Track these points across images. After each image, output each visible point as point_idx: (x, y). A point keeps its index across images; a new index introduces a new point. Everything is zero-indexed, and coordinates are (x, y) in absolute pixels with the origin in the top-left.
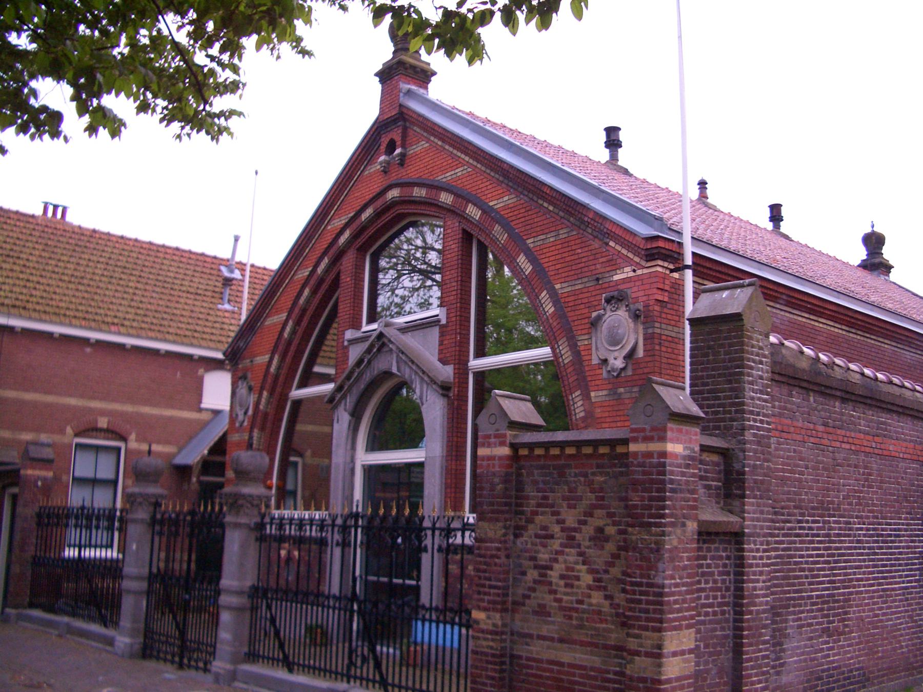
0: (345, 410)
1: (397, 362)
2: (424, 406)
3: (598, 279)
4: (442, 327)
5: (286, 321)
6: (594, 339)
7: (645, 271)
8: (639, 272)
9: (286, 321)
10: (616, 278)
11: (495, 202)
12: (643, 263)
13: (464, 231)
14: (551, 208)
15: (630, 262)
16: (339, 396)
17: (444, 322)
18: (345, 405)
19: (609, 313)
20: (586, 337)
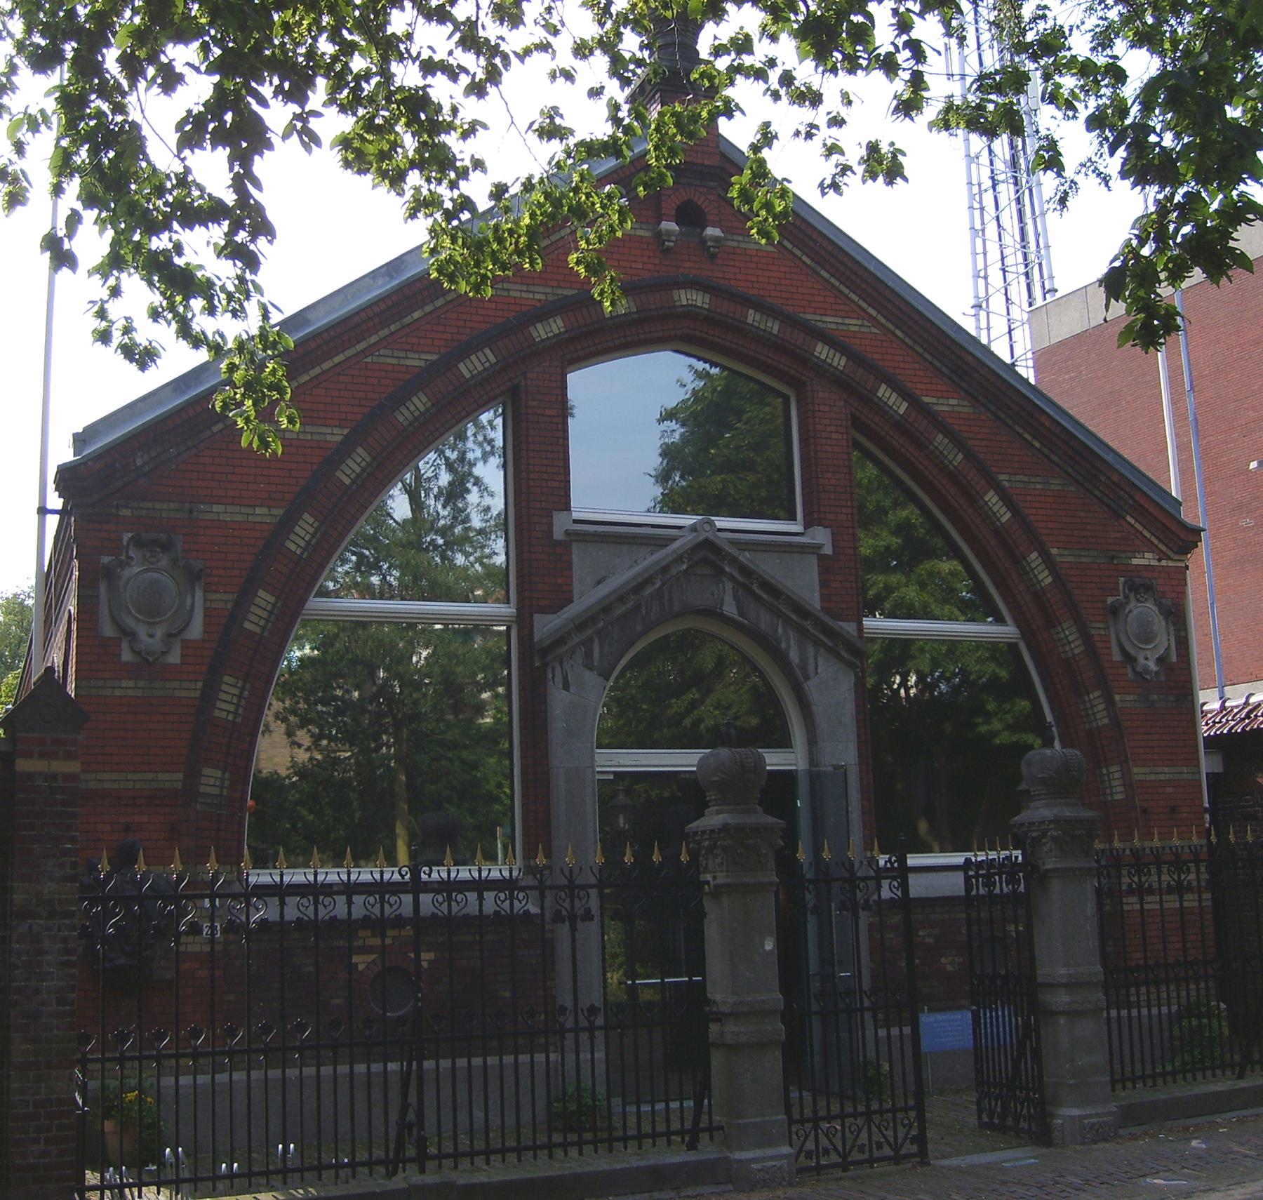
0: (589, 666)
1: (736, 598)
2: (810, 682)
3: (1113, 557)
4: (822, 558)
5: (345, 449)
6: (1112, 630)
7: (1171, 563)
8: (1164, 563)
9: (345, 449)
10: (1135, 562)
11: (934, 400)
12: (1170, 554)
13: (852, 415)
14: (1037, 445)
15: (1152, 548)
16: (576, 640)
17: (828, 550)
18: (589, 654)
19: (1133, 604)
20: (1101, 625)
